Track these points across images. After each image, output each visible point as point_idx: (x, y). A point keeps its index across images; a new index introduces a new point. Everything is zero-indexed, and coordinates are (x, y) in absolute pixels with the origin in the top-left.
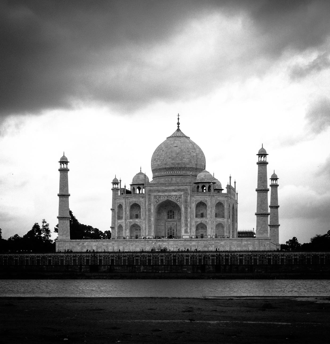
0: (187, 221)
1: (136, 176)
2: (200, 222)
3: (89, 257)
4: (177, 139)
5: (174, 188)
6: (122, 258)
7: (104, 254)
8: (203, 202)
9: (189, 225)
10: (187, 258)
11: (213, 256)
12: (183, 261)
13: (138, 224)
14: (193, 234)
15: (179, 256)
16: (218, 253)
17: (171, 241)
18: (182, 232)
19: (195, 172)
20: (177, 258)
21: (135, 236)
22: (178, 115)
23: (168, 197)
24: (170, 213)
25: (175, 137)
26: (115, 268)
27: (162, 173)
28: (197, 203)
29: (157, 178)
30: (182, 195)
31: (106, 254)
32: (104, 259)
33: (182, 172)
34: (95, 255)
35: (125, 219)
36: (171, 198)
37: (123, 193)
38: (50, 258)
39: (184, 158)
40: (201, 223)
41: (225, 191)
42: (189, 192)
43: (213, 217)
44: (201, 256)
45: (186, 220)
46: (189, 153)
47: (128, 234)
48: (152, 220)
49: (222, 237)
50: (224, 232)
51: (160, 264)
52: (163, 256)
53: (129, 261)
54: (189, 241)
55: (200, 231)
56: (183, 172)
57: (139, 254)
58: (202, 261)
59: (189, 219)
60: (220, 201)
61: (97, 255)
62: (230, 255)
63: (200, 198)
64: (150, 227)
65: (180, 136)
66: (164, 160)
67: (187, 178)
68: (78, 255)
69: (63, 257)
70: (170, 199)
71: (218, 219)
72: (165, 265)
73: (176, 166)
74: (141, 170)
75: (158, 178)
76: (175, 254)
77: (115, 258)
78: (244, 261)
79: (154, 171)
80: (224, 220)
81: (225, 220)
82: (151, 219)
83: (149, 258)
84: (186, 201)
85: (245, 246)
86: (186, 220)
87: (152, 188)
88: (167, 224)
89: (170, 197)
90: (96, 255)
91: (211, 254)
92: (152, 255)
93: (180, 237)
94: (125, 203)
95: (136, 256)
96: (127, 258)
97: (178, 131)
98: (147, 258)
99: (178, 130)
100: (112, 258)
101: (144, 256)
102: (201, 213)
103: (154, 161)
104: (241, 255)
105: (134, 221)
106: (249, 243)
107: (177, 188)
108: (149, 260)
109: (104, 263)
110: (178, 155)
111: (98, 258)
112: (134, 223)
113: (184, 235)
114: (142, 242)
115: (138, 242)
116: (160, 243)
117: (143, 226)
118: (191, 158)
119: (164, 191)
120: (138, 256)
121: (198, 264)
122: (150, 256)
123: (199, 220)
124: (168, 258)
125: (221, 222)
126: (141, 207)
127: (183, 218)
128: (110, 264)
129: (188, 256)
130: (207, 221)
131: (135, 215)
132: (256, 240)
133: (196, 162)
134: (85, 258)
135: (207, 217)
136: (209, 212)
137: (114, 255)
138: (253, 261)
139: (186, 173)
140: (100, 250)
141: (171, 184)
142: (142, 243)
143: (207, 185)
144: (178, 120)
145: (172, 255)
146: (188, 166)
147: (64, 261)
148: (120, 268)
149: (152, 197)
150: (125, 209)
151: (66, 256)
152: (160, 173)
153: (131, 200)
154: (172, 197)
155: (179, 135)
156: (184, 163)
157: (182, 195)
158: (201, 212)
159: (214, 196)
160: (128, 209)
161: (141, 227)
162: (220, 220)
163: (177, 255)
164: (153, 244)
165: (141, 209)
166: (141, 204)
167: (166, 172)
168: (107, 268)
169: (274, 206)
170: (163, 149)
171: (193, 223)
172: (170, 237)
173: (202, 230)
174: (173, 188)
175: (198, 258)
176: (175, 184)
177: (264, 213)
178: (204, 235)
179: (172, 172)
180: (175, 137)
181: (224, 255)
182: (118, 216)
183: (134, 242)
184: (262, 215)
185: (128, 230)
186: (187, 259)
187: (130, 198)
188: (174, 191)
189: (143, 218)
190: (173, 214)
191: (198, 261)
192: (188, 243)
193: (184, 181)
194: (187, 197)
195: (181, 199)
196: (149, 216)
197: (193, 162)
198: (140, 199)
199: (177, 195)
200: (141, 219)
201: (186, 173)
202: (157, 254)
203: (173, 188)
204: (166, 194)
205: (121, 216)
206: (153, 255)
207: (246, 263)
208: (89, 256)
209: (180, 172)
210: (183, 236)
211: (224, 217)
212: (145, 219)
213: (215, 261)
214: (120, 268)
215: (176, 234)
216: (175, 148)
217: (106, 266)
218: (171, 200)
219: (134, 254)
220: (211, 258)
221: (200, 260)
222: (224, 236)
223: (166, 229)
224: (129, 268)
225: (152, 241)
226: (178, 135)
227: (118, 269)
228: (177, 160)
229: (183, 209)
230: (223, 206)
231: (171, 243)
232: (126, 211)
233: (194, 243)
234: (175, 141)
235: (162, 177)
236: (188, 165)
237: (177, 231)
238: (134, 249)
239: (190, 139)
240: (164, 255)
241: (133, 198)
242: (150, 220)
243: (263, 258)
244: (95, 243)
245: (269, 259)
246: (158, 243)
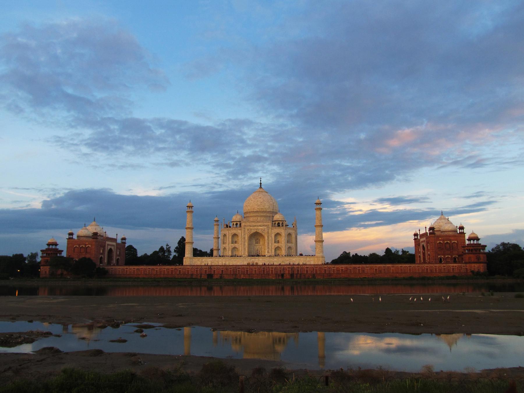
11: (289, 268)
41: (291, 226)
42: (270, 226)
64: (245, 249)
84: (268, 233)
85: (308, 261)
101: (243, 268)
108: (247, 271)
116: (254, 260)
119: (254, 226)
123: (277, 245)
127: (266, 244)
140: (213, 264)
141: (258, 222)
143: (281, 223)
149: (246, 230)
160: (230, 237)
162: (289, 245)
171: (273, 247)
174: (260, 224)
203: (260, 224)
204: (255, 228)
221: (280, 271)
229: (266, 238)
233: (275, 259)
242: (244, 245)
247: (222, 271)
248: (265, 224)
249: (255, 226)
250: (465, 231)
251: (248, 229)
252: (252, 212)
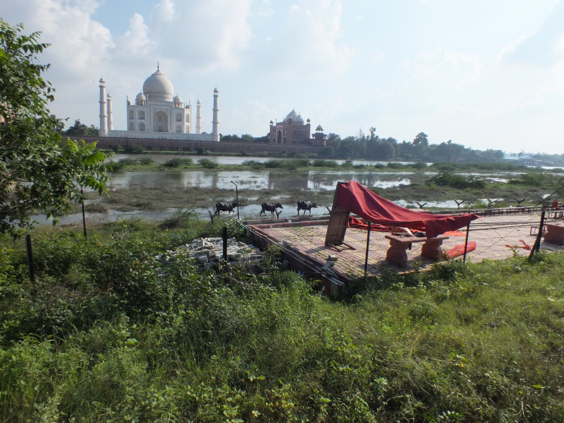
84: (171, 112)
93: (167, 131)
119: (159, 105)
123: (178, 123)
172: (160, 131)
250: (311, 123)
251: (153, 108)
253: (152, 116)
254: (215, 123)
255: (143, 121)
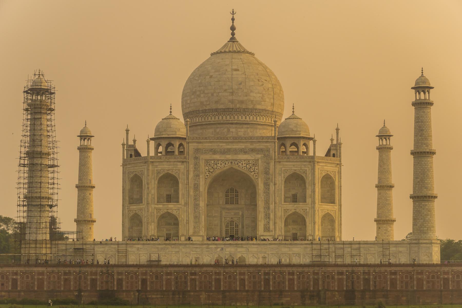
0: (269, 208)
1: (161, 122)
2: (293, 211)
3: (96, 275)
4: (235, 55)
5: (243, 147)
6: (164, 277)
7: (126, 269)
8: (299, 173)
9: (272, 216)
10: (291, 277)
11: (341, 273)
12: (284, 283)
13: (174, 213)
14: (280, 233)
15: (275, 273)
16: (350, 269)
17: (253, 246)
18: (260, 229)
19: (270, 119)
20: (271, 277)
21: (165, 235)
22: (233, 12)
23: (231, 162)
24: (229, 194)
25: (230, 52)
26: (150, 296)
27: (210, 118)
28: (287, 175)
29: (199, 127)
30: (260, 161)
31: (131, 269)
32: (128, 279)
33: (248, 117)
34: (108, 270)
35: (148, 204)
36: (237, 165)
37: (133, 154)
38: (15, 277)
39: (251, 92)
40: (295, 213)
43: (317, 201)
44: (317, 274)
45: (267, 207)
46: (260, 83)
47: (153, 232)
48: (201, 205)
49: (329, 239)
50: (333, 230)
51: (238, 289)
52: (244, 274)
53: (177, 283)
54: (287, 246)
55: (290, 227)
56: (249, 119)
57: (197, 270)
58: (320, 283)
59: (272, 204)
60: (329, 173)
61: (113, 272)
62: (372, 271)
63: (294, 165)
64: (197, 218)
65: (239, 52)
66: (215, 94)
67: (257, 128)
68: (74, 271)
69: (42, 274)
70: (236, 167)
71: (326, 206)
72: (247, 291)
73: (238, 106)
74: (171, 112)
75: (201, 129)
76: (267, 270)
77: (149, 277)
78: (398, 282)
79: (186, 115)
80: (334, 208)
81: (336, 207)
82: (199, 204)
83: (218, 277)
84: (267, 173)
86: (267, 207)
87: (200, 146)
88: (224, 214)
89: (236, 163)
90: (110, 272)
91: (336, 269)
92: (222, 271)
94: (148, 173)
95: (192, 274)
96: (173, 277)
97: (233, 42)
98: (213, 277)
99: (233, 39)
100: (144, 277)
102: (293, 195)
103: (193, 97)
104: (393, 271)
105: (166, 206)
106: (401, 249)
107: (250, 146)
108: (218, 281)
109: (127, 287)
110: (241, 86)
111: (115, 277)
112: (166, 211)
113: (262, 234)
114: (195, 246)
115: (188, 246)
117: (183, 217)
118: (264, 92)
119: (224, 152)
120: (195, 274)
121: (312, 289)
122: (219, 274)
123: (291, 207)
124: (254, 277)
125: (329, 212)
126: (180, 181)
127: (261, 204)
128: (140, 289)
129: (293, 274)
130: (306, 209)
131: (165, 196)
132: (412, 245)
133: (272, 101)
134: (89, 277)
135: (305, 201)
136: (309, 192)
137: (146, 271)
138: (415, 283)
139: (255, 119)
141: (237, 139)
142: (197, 248)
144: (233, 22)
145: (262, 272)
146: (258, 107)
147: (45, 283)
148: (158, 296)
149: (202, 163)
150: (148, 184)
151: (50, 273)
152: (205, 119)
153: (160, 168)
154: (239, 164)
155: (232, 47)
156: (252, 101)
157: (258, 160)
158: (293, 192)
159: (318, 162)
161: (180, 219)
162: (328, 208)
163: (271, 271)
164: (219, 250)
165: (180, 185)
166: (180, 176)
167: (217, 117)
168: (133, 296)
169: (386, 186)
170: (211, 74)
171: (280, 213)
172: (232, 237)
173: (295, 227)
175: (311, 277)
176: (245, 138)
177: (429, 195)
178: (298, 234)
179: (228, 117)
180: (230, 52)
181: (362, 271)
182: (129, 197)
183: (181, 247)
184: (425, 199)
185: (153, 224)
186: (290, 280)
187: (157, 164)
188: (244, 152)
189: (183, 201)
190: (237, 196)
191: (312, 283)
192: (287, 249)
193: (251, 134)
194: (268, 164)
195: (256, 168)
196: (196, 199)
197: (267, 100)
198: (179, 166)
199: (249, 160)
200: (180, 203)
201: (255, 119)
202: (232, 270)
204: (229, 157)
205: (135, 197)
206: (224, 272)
207: (402, 287)
208: (96, 274)
209: (244, 117)
210: (260, 236)
211: (333, 202)
212: (186, 204)
213: (345, 283)
214: (158, 296)
215: (243, 233)
216: (235, 73)
217: (132, 293)
218: (239, 169)
219: (189, 270)
220: (336, 277)
221: (316, 282)
222: (335, 237)
223: (223, 224)
224: (177, 296)
225: (216, 244)
226: (235, 49)
227: (156, 298)
228: (240, 95)
229: (261, 187)
230: (333, 183)
231: (254, 249)
232: (150, 189)
233: (296, 249)
234: (233, 60)
235: (208, 126)
236: (259, 104)
237: (243, 227)
238: (181, 260)
239: (255, 56)
240: (246, 272)
241: (165, 163)
242: (196, 206)
243: (433, 277)
244: (103, 247)
245: (444, 279)
246: (228, 250)
247: (144, 282)
248: (257, 146)
249: (228, 151)
251: (207, 161)
252: (211, 110)
253: (203, 188)
254: (422, 198)
255: (171, 206)
